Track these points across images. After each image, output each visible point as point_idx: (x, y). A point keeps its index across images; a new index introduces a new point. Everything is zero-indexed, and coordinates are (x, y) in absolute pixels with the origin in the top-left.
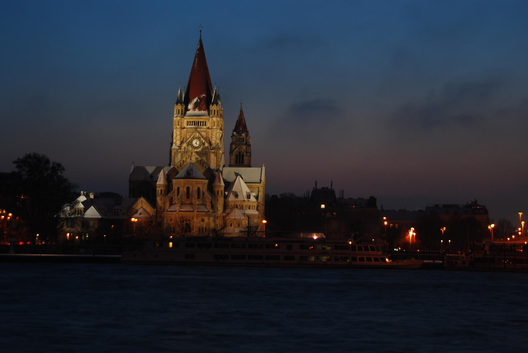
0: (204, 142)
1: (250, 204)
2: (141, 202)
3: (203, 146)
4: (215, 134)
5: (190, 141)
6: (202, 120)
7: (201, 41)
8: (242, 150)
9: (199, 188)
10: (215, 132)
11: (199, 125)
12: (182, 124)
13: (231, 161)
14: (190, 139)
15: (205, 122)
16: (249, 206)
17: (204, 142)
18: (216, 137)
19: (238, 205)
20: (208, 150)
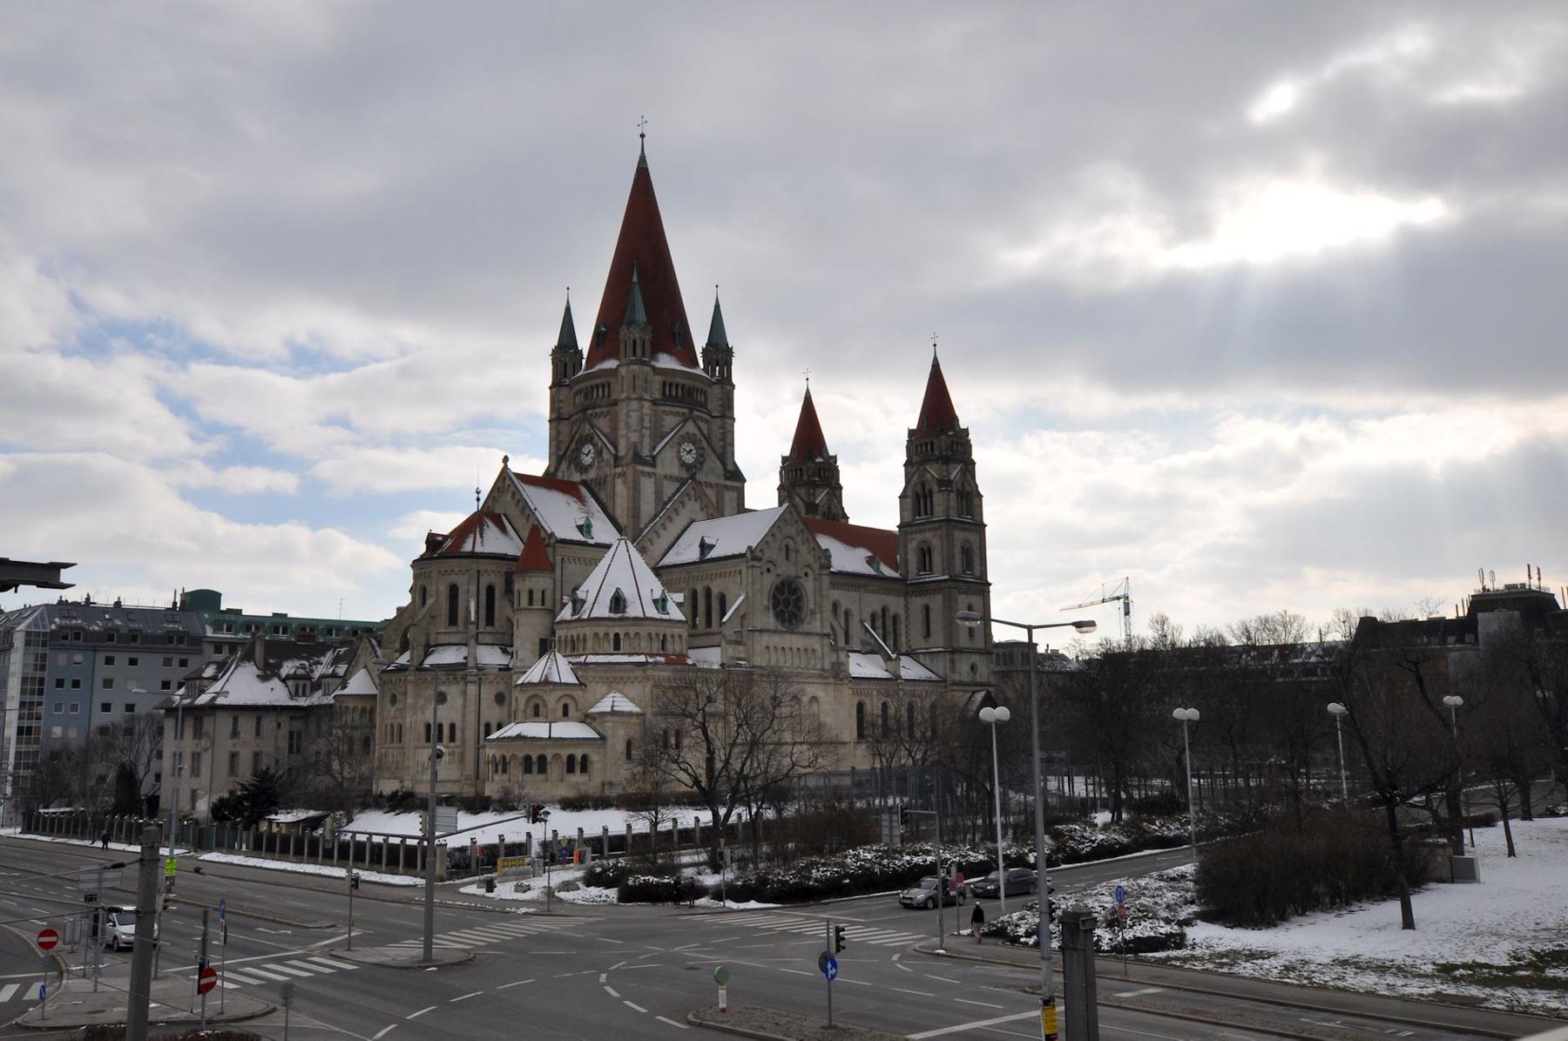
0: (601, 448)
1: (617, 630)
2: (364, 652)
3: (598, 462)
4: (624, 418)
5: (573, 451)
6: (598, 381)
7: (643, 160)
8: (929, 476)
9: (454, 591)
10: (625, 411)
11: (592, 398)
12: (561, 405)
13: (903, 514)
14: (573, 446)
15: (609, 384)
16: (612, 636)
17: (601, 448)
18: (628, 425)
19: (575, 639)
20: (607, 471)
